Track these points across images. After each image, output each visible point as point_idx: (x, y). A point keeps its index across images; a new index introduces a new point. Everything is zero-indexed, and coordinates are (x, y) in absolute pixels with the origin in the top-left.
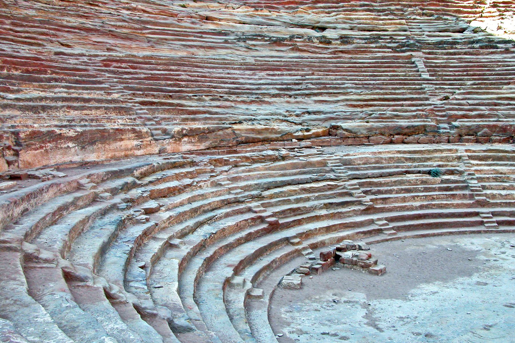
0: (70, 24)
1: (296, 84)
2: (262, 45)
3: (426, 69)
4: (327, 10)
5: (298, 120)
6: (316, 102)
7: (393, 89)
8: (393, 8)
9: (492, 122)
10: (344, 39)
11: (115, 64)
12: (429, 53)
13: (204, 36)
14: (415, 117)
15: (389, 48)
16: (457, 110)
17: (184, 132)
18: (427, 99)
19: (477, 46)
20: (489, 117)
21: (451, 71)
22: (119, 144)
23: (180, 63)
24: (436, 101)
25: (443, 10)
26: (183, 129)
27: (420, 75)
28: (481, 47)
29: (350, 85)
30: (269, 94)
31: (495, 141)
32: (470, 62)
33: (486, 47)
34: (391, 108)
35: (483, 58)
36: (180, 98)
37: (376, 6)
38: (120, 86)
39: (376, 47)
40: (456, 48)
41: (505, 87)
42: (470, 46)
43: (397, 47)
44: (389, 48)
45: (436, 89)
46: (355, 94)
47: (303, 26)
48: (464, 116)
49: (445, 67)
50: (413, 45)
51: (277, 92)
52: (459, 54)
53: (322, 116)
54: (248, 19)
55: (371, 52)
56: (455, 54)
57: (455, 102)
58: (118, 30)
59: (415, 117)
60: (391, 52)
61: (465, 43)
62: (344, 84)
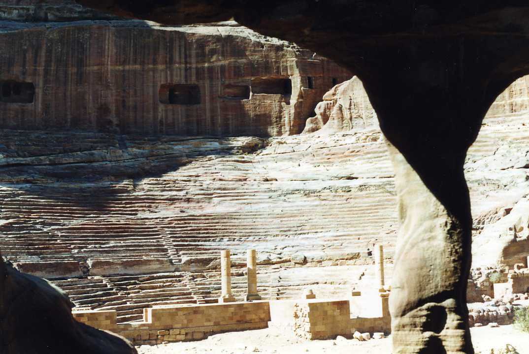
0: (162, 198)
2: (296, 197)
4: (371, 161)
5: (279, 251)
10: (362, 187)
11: (176, 222)
13: (256, 194)
15: (390, 192)
17: (192, 260)
22: (148, 267)
23: (223, 217)
26: (191, 259)
30: (271, 235)
36: (205, 241)
38: (169, 236)
44: (390, 192)
51: (278, 233)
55: (373, 197)
58: (195, 197)
59: (359, 247)
60: (389, 196)
62: (330, 225)
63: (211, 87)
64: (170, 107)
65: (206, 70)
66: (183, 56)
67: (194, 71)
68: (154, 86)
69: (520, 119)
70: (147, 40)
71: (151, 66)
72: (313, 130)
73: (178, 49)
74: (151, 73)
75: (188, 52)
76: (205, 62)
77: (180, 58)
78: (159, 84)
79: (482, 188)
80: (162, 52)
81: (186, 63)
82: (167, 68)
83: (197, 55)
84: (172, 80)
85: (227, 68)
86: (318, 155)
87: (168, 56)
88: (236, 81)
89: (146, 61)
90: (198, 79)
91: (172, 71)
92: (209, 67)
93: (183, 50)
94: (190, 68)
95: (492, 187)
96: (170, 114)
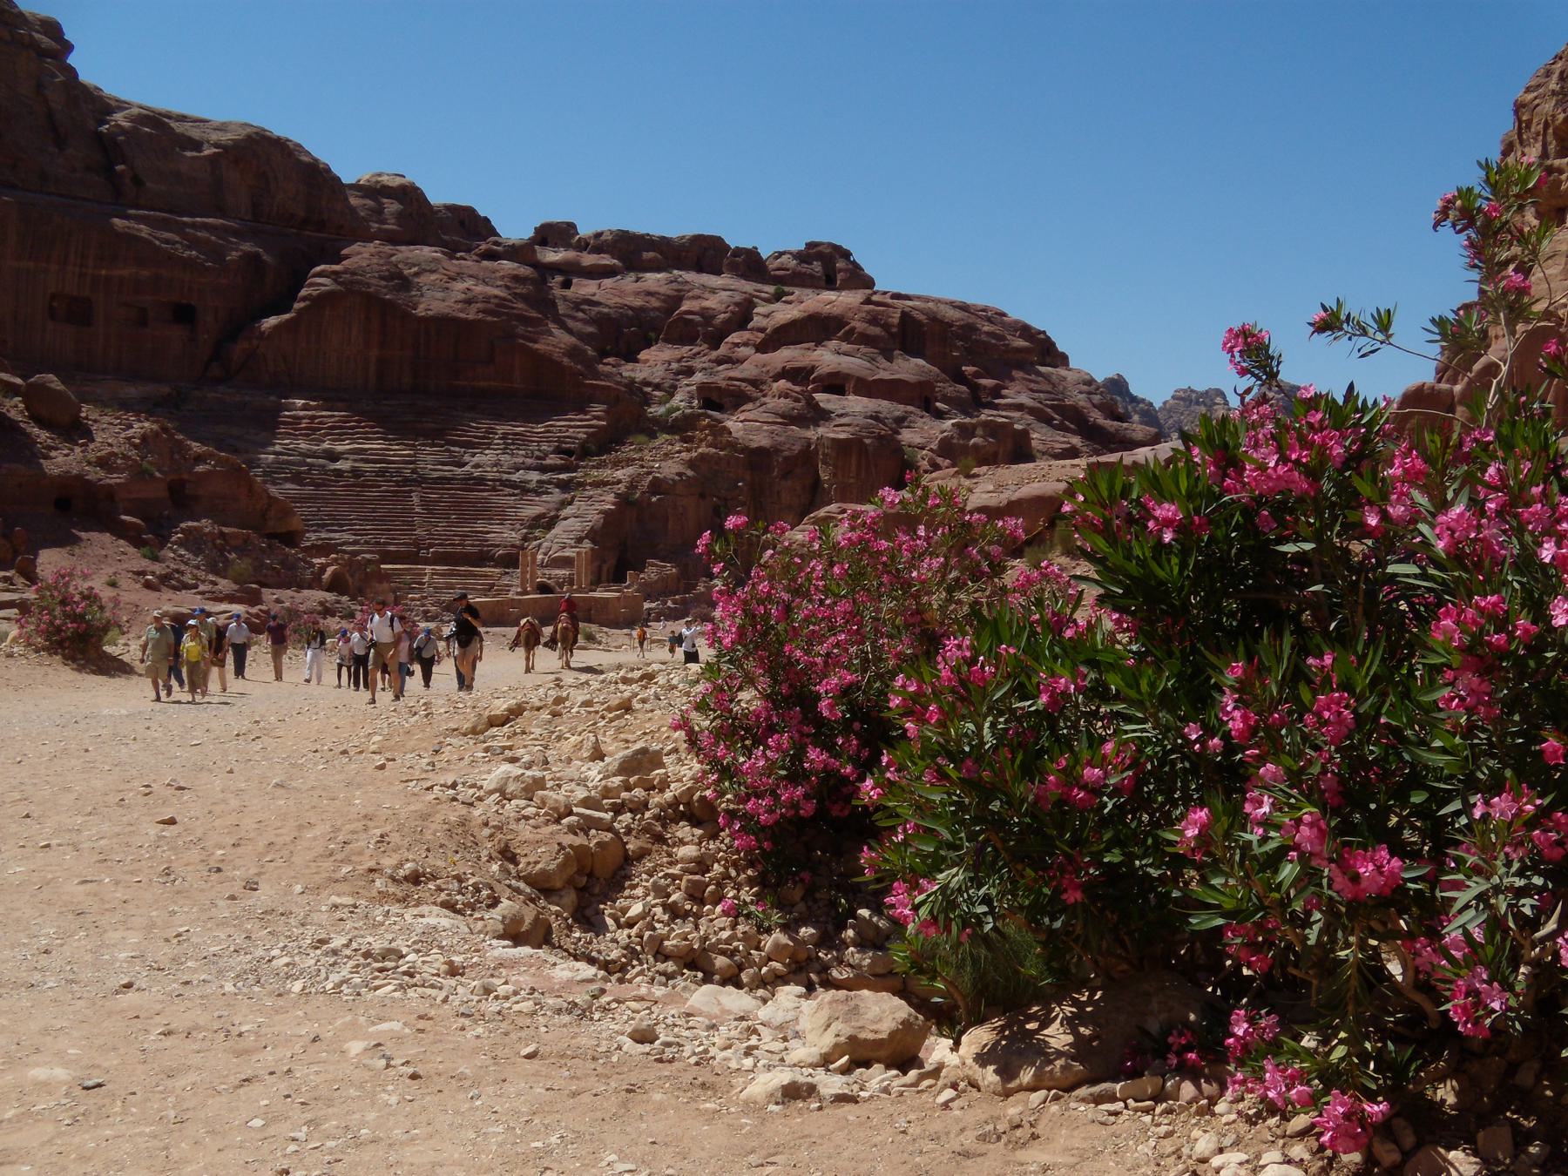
10: (355, 472)
79: (508, 490)
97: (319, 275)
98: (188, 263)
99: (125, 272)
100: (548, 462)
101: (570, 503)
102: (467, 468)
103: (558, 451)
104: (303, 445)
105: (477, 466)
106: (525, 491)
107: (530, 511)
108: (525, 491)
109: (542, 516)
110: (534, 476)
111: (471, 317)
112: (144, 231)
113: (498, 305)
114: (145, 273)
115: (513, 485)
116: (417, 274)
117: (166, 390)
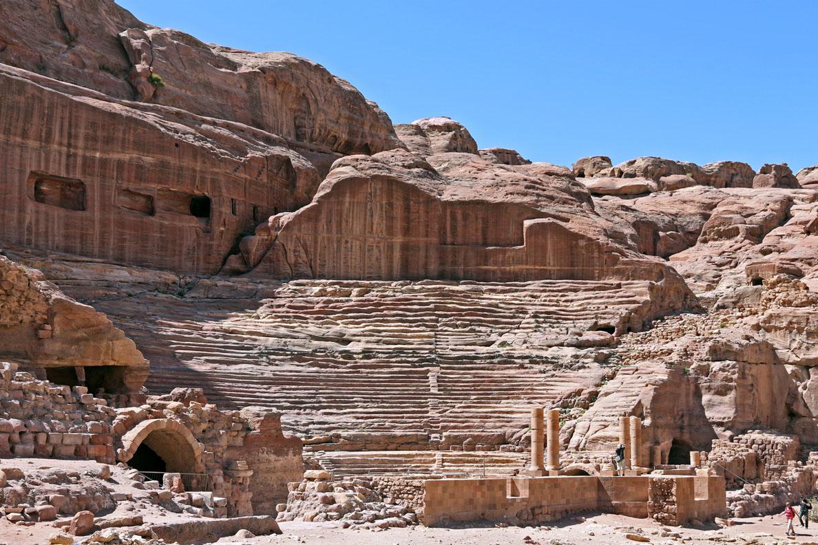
1: (307, 398)
3: (437, 384)
6: (325, 414)
7: (399, 403)
8: (425, 318)
9: (476, 432)
10: (367, 353)
12: (447, 368)
14: (410, 427)
15: (408, 362)
16: (451, 422)
18: (427, 412)
19: (495, 361)
20: (477, 428)
21: (461, 386)
24: (433, 414)
25: (481, 321)
27: (429, 390)
28: (499, 363)
29: (359, 399)
31: (479, 449)
32: (483, 377)
33: (505, 362)
34: (390, 420)
35: (497, 374)
37: (410, 316)
39: (396, 362)
40: (475, 363)
41: (503, 401)
42: (488, 361)
43: (416, 362)
44: (408, 362)
45: (440, 403)
46: (361, 407)
47: (327, 339)
48: (455, 427)
49: (456, 382)
50: (433, 360)
51: (289, 404)
52: (476, 369)
53: (326, 426)
54: (273, 332)
56: (472, 369)
57: (451, 415)
59: (410, 427)
61: (486, 358)
62: (353, 398)
63: (103, 187)
64: (43, 207)
65: (97, 162)
66: (65, 133)
67: (79, 161)
68: (21, 172)
69: (525, 290)
70: (17, 98)
71: (18, 139)
72: (237, 273)
73: (58, 124)
74: (18, 150)
75: (73, 130)
76: (95, 150)
77: (61, 136)
78: (28, 171)
79: (537, 367)
80: (35, 119)
81: (69, 145)
82: (41, 147)
83: (87, 138)
84: (47, 167)
85: (126, 166)
86: (279, 306)
87: (44, 130)
88: (137, 186)
89: (12, 128)
90: (84, 172)
91: (48, 154)
92: (101, 159)
93: (66, 124)
94: (75, 155)
95: (550, 367)
96: (42, 217)
97: (339, 165)
98: (196, 152)
99: (126, 157)
100: (584, 338)
101: (612, 377)
102: (493, 348)
103: (595, 327)
104: (312, 329)
105: (503, 344)
106: (558, 366)
107: (563, 389)
108: (558, 366)
109: (579, 393)
110: (570, 351)
111: (499, 200)
112: (151, 118)
113: (527, 187)
114: (149, 159)
115: (545, 361)
116: (446, 169)
117: (171, 277)
